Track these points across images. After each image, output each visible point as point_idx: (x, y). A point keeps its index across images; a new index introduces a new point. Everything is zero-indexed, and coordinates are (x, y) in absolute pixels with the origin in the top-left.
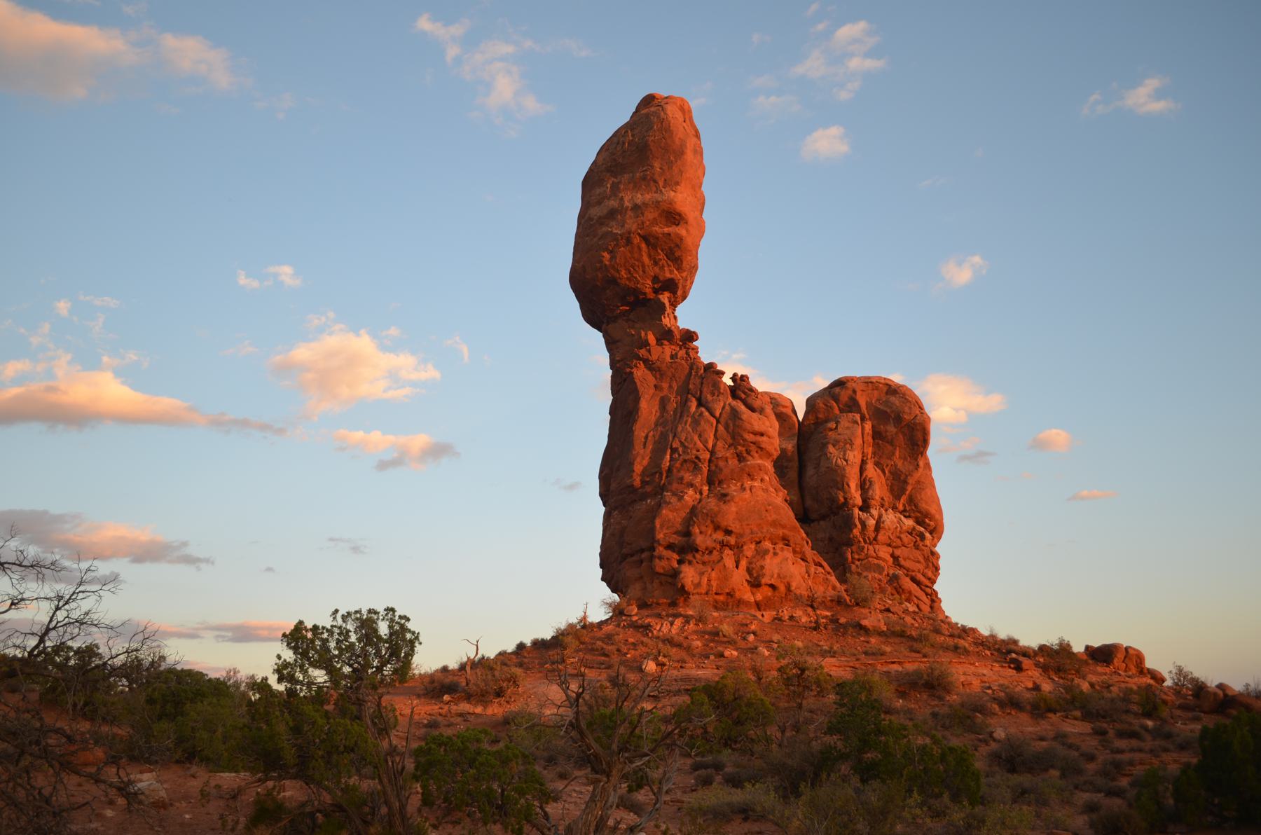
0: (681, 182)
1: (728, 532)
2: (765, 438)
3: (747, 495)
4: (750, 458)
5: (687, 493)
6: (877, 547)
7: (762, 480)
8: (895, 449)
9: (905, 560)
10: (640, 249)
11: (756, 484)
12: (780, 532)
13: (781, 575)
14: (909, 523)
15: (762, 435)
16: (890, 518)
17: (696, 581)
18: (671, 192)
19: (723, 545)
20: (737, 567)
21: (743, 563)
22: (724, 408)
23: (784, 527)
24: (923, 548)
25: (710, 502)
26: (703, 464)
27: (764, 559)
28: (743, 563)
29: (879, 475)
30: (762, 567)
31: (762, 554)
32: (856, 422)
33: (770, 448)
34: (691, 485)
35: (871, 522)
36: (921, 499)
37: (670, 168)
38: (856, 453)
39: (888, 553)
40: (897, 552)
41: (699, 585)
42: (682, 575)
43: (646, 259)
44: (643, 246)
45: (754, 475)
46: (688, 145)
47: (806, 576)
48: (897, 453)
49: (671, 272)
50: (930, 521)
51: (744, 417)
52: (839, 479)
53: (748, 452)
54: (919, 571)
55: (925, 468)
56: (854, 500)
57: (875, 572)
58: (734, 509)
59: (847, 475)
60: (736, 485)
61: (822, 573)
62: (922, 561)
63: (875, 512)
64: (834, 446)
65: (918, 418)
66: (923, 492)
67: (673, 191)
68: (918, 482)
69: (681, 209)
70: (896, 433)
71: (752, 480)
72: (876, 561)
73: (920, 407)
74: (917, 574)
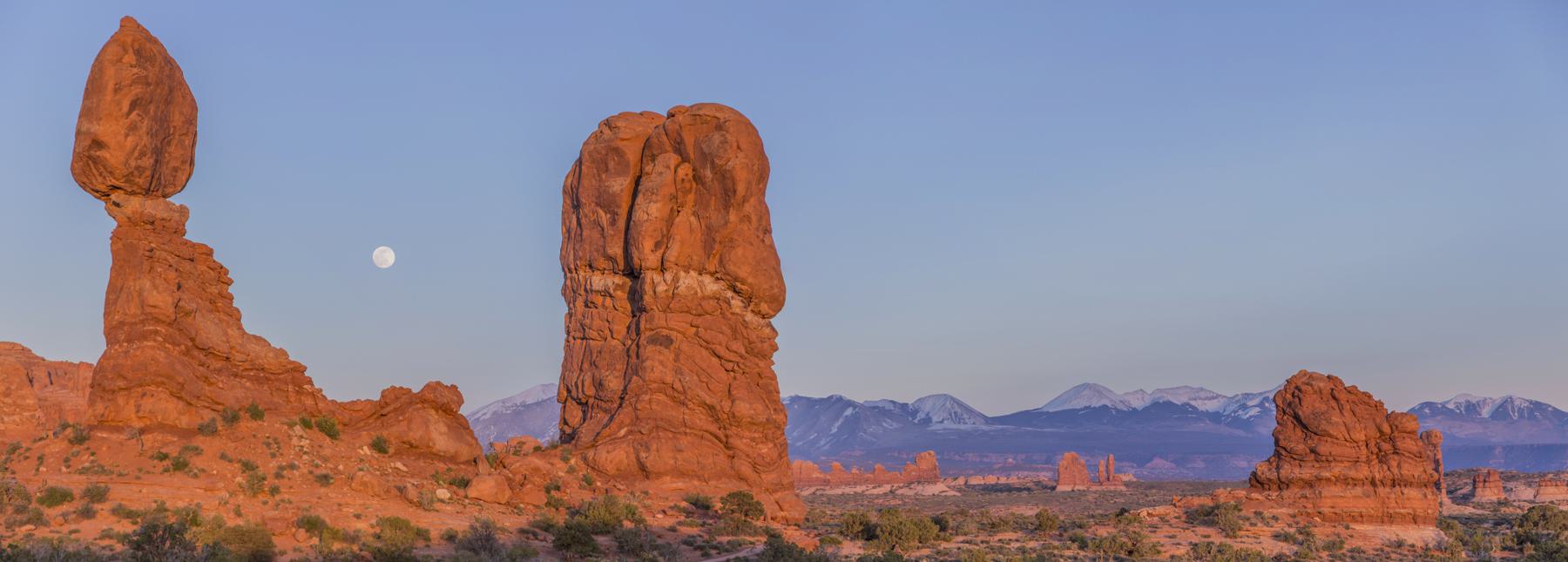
2: (157, 310)
3: (138, 353)
6: (670, 315)
7: (155, 340)
8: (711, 199)
9: (706, 330)
10: (88, 164)
11: (149, 344)
12: (159, 379)
14: (711, 286)
15: (154, 307)
16: (688, 281)
17: (102, 412)
21: (132, 402)
24: (730, 316)
28: (132, 402)
29: (691, 231)
30: (140, 406)
31: (144, 395)
32: (668, 167)
35: (661, 288)
36: (730, 260)
38: (659, 205)
39: (687, 323)
40: (698, 321)
41: (103, 415)
43: (94, 171)
44: (90, 162)
48: (713, 202)
50: (743, 284)
52: (636, 236)
54: (720, 344)
55: (741, 221)
56: (646, 263)
57: (661, 345)
59: (643, 233)
61: (204, 407)
62: (729, 332)
63: (668, 276)
64: (644, 195)
65: (730, 163)
66: (734, 252)
68: (731, 240)
70: (712, 180)
72: (665, 332)
73: (739, 147)
74: (718, 347)
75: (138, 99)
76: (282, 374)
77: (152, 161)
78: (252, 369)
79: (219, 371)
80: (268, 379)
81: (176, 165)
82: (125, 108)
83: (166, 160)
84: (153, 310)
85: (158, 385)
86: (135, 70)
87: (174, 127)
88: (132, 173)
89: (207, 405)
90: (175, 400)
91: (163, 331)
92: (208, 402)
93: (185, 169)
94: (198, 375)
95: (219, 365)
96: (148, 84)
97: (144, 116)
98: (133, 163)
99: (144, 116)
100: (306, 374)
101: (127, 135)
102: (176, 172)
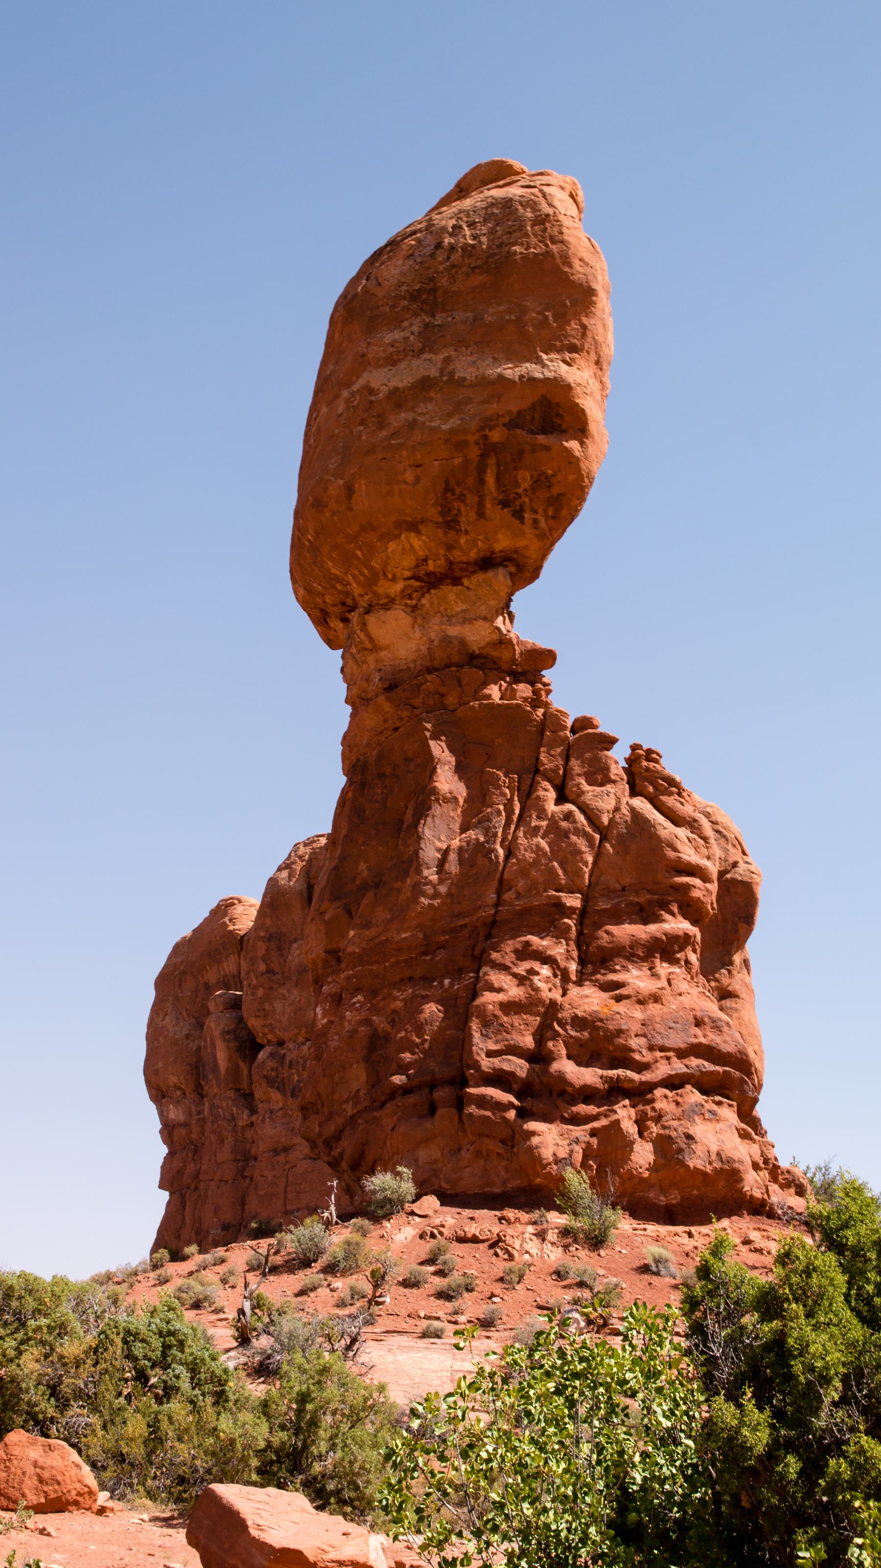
1: (623, 1059)
2: (697, 882)
5: (538, 974)
22: (617, 809)
25: (587, 997)
49: (536, 522)
67: (565, 362)
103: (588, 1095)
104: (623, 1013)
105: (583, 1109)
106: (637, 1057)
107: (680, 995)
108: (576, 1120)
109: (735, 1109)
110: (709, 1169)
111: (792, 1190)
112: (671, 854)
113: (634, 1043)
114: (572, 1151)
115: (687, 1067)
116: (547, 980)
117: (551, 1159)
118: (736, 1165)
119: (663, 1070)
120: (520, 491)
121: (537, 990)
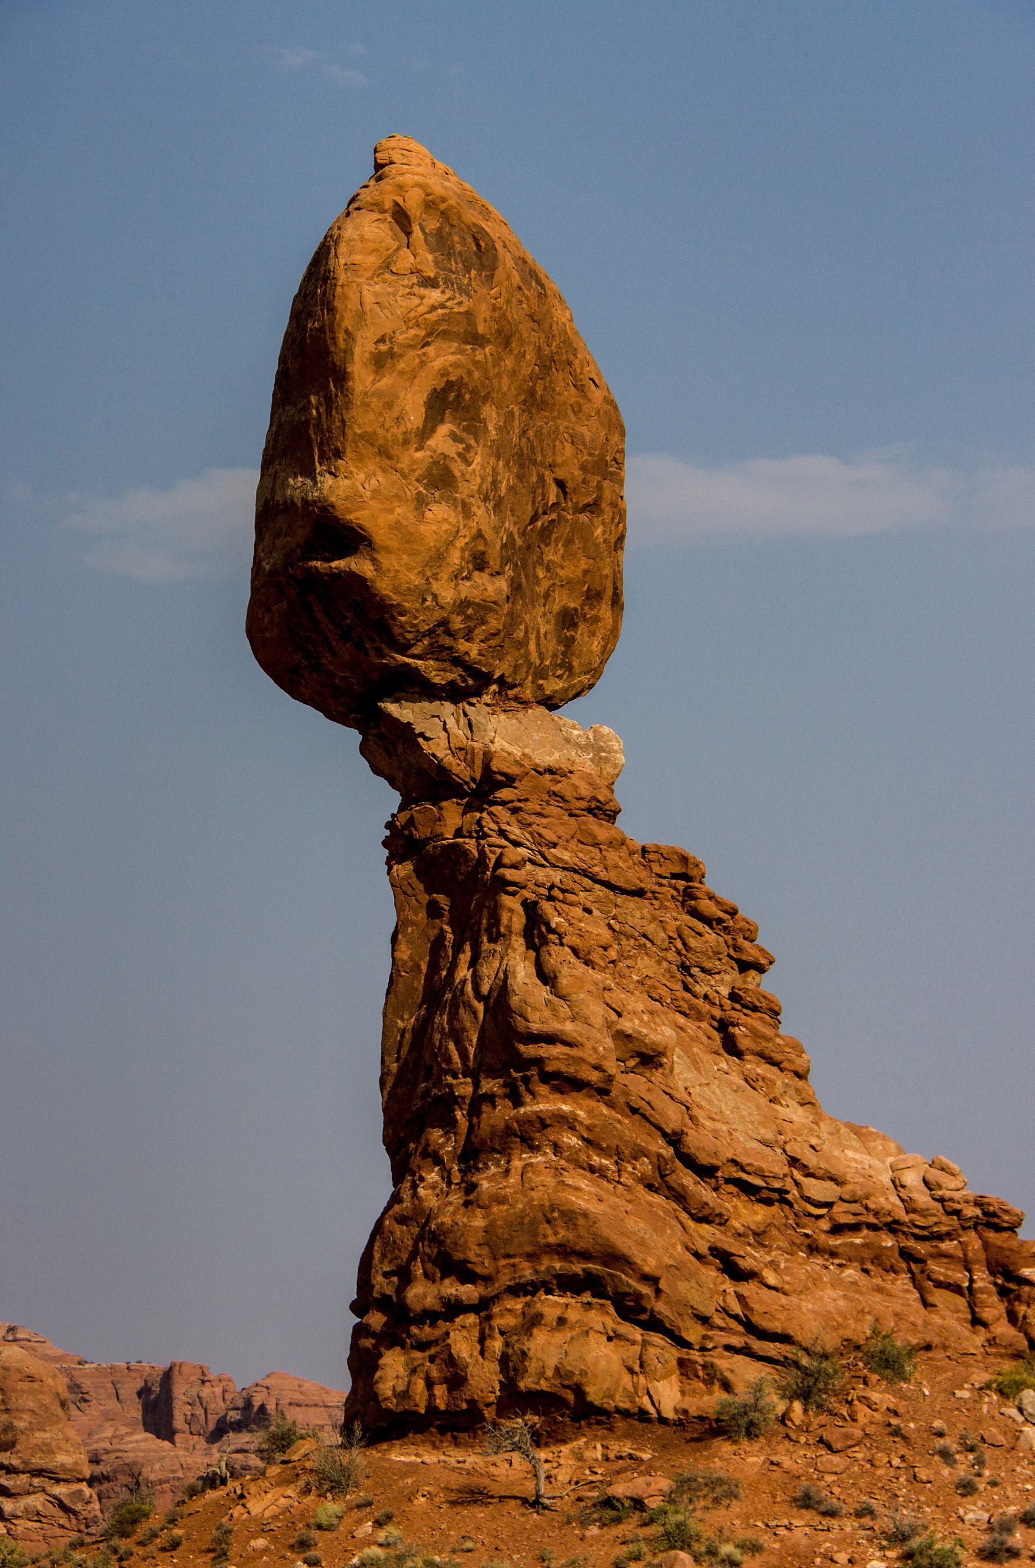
0: (344, 447)
2: (557, 1050)
4: (528, 1098)
7: (557, 1148)
12: (578, 1267)
13: (562, 1372)
17: (400, 1388)
18: (327, 475)
19: (453, 1309)
20: (482, 1353)
21: (497, 1345)
23: (585, 1256)
26: (461, 1109)
27: (531, 1335)
28: (497, 1345)
31: (532, 1321)
33: (572, 1069)
34: (437, 1160)
37: (329, 412)
41: (404, 1395)
42: (378, 1374)
45: (532, 1139)
46: (357, 351)
47: (637, 1369)
51: (514, 1001)
53: (526, 1080)
58: (479, 1222)
60: (498, 1165)
61: (728, 1348)
67: (331, 473)
69: (351, 517)
71: (534, 1149)
75: (450, 385)
76: (949, 1236)
77: (502, 585)
78: (855, 1228)
79: (759, 1237)
80: (905, 1254)
81: (572, 605)
82: (415, 418)
83: (540, 589)
84: (543, 1050)
85: (570, 1284)
86: (435, 295)
87: (561, 484)
88: (444, 623)
89: (737, 1341)
90: (637, 1334)
91: (581, 1114)
92: (736, 1333)
93: (596, 619)
94: (703, 1248)
95: (759, 1218)
96: (475, 339)
97: (472, 442)
98: (447, 594)
99: (472, 442)
100: (1022, 1233)
101: (421, 503)
102: (574, 625)
103: (430, 1317)
104: (460, 1223)
105: (425, 1332)
106: (479, 1270)
107: (532, 1189)
108: (422, 1346)
109: (612, 1310)
110: (544, 1385)
111: (717, 1386)
112: (521, 1025)
113: (471, 1256)
114: (409, 1382)
115: (536, 1272)
116: (433, 1187)
117: (389, 1393)
118: (577, 1378)
119: (505, 1280)
120: (348, 621)
121: (419, 1199)
